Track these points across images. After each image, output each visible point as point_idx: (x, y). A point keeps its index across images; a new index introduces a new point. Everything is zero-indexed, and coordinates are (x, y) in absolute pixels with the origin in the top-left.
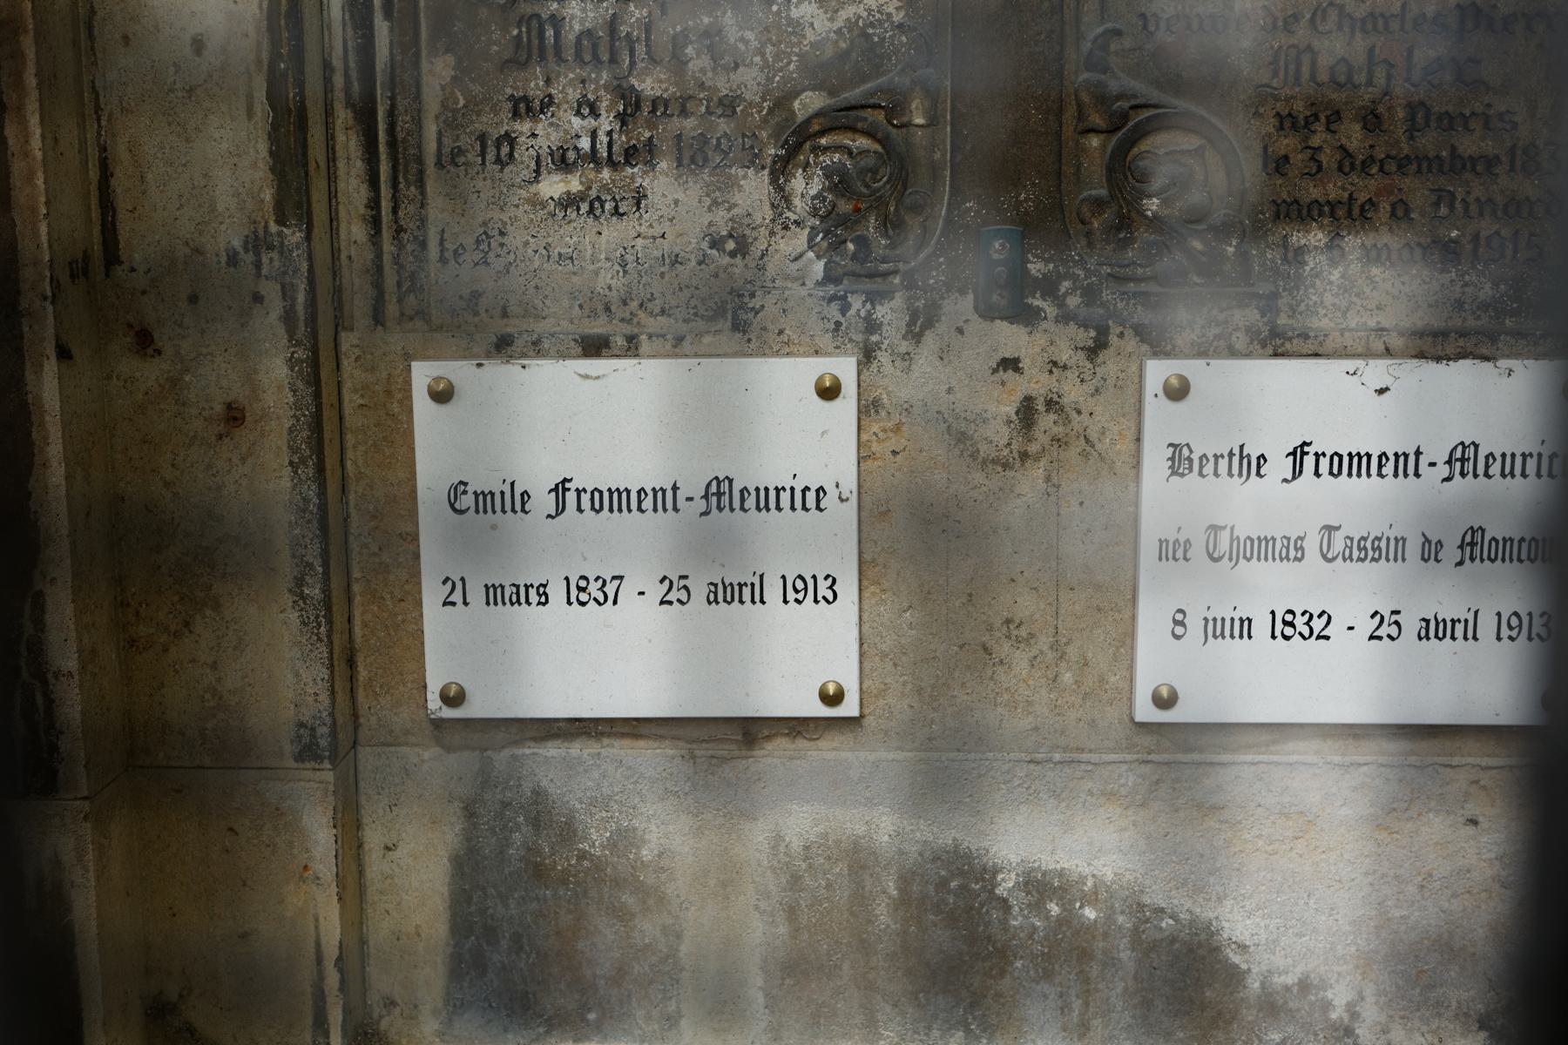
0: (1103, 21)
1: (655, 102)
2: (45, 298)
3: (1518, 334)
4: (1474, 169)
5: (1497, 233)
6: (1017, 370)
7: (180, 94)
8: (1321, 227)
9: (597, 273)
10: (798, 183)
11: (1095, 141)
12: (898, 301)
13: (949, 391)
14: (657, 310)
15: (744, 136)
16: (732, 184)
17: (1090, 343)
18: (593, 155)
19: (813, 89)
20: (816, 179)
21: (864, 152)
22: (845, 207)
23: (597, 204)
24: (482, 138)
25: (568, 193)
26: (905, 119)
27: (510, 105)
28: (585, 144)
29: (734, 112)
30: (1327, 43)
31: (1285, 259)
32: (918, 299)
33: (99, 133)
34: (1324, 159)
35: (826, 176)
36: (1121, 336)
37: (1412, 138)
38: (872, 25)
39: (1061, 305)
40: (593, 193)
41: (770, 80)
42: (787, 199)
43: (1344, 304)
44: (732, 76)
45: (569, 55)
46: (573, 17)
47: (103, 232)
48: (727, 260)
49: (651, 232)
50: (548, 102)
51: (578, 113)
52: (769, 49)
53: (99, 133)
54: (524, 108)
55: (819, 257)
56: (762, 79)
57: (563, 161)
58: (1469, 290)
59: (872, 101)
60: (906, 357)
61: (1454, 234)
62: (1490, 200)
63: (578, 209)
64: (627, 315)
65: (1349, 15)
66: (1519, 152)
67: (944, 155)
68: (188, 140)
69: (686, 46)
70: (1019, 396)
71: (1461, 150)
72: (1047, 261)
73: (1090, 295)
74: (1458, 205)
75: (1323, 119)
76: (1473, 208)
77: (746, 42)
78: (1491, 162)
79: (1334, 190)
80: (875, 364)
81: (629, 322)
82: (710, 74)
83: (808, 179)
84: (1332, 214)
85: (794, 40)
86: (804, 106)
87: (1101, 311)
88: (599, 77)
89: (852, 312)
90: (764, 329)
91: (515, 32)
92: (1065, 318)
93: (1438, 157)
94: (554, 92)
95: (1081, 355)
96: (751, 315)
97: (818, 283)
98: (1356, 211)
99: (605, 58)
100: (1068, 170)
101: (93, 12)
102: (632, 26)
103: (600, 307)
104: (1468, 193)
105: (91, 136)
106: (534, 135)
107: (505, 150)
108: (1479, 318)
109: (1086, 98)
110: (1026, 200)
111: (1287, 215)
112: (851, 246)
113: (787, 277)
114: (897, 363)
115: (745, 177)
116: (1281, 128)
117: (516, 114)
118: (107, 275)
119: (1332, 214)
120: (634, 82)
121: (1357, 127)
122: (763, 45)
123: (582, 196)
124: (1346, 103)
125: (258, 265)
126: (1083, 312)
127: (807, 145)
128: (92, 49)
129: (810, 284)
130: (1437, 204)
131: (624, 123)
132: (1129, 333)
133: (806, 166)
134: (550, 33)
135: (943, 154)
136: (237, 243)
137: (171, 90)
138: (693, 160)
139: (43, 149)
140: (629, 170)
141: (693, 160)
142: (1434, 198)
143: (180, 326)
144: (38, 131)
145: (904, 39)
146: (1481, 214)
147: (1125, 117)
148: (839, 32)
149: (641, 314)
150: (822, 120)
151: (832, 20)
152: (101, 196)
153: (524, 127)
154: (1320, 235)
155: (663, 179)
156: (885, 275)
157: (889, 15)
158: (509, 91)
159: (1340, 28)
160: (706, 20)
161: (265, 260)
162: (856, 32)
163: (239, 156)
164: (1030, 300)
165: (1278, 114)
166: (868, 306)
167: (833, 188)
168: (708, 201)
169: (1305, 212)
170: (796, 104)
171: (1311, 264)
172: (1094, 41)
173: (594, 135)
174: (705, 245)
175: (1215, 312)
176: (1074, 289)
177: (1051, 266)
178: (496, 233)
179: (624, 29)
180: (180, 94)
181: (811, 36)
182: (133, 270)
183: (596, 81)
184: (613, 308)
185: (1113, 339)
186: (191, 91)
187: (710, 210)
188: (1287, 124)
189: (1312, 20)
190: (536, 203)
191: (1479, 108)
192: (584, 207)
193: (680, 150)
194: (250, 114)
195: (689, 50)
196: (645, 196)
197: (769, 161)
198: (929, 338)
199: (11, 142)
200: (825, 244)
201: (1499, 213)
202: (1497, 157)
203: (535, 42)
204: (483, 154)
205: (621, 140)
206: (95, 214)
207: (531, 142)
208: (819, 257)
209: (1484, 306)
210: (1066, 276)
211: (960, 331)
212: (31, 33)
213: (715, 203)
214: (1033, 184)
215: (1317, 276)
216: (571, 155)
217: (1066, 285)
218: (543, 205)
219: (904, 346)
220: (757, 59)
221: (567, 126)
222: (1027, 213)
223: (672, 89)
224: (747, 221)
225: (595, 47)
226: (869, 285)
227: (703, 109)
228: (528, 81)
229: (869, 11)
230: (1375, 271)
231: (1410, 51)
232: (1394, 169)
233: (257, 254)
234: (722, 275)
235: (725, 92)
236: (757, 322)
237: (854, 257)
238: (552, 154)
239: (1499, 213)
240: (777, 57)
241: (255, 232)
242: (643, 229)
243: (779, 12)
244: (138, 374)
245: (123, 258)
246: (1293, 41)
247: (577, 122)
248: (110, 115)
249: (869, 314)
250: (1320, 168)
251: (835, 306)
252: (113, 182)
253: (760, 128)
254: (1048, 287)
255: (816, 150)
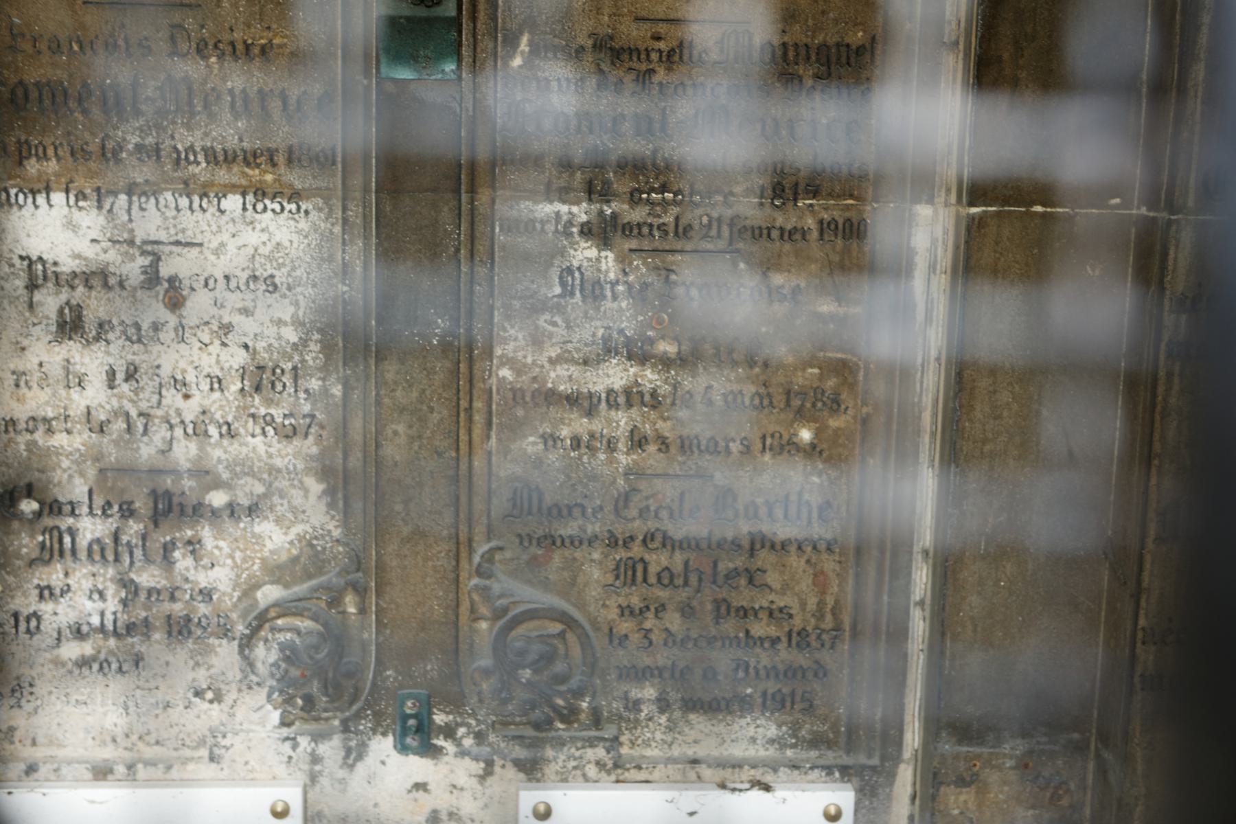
0: (489, 539)
1: (150, 592)
3: (795, 767)
4: (762, 644)
5: (780, 691)
6: (426, 790)
8: (652, 685)
9: (105, 714)
10: (260, 651)
11: (484, 625)
12: (337, 740)
13: (376, 805)
14: (153, 741)
15: (219, 616)
16: (210, 650)
17: (481, 772)
18: (102, 629)
19: (272, 583)
20: (273, 651)
21: (310, 633)
22: (295, 673)
23: (105, 665)
24: (16, 616)
25: (83, 656)
26: (341, 609)
27: (37, 592)
28: (96, 620)
29: (211, 599)
30: (654, 557)
31: (626, 708)
32: (350, 740)
34: (653, 637)
35: (282, 650)
36: (503, 766)
37: (717, 623)
38: (316, 538)
39: (459, 745)
40: (102, 656)
41: (238, 576)
42: (251, 665)
43: (669, 739)
44: (209, 572)
45: (83, 555)
46: (85, 529)
48: (206, 705)
49: (147, 685)
50: (67, 589)
51: (90, 598)
52: (238, 555)
54: (46, 593)
55: (275, 708)
56: (232, 575)
57: (78, 633)
58: (760, 730)
59: (315, 595)
60: (342, 781)
61: (749, 691)
62: (774, 667)
63: (91, 667)
64: (129, 745)
65: (671, 538)
66: (794, 635)
67: (370, 635)
69: (174, 550)
70: (427, 810)
71: (753, 632)
72: (448, 713)
73: (480, 737)
74: (751, 670)
75: (653, 609)
76: (763, 673)
77: (220, 549)
78: (775, 641)
79: (662, 658)
80: (317, 788)
81: (131, 750)
82: (192, 572)
83: (268, 649)
84: (660, 676)
85: (257, 547)
86: (265, 595)
87: (488, 749)
88: (106, 572)
89: (300, 749)
90: (234, 761)
91: (40, 538)
92: (462, 753)
93: (736, 637)
94: (70, 582)
95: (474, 781)
96: (223, 751)
97: (275, 727)
98: (677, 675)
99: (111, 558)
100: (463, 647)
102: (131, 536)
103: (108, 739)
104: (758, 662)
106: (55, 614)
107: (33, 623)
108: (767, 749)
109: (476, 597)
110: (432, 670)
111: (628, 676)
112: (300, 702)
113: (251, 722)
114: (337, 786)
115: (220, 645)
116: (622, 615)
117: (41, 596)
119: (660, 676)
120: (133, 576)
121: (677, 615)
122: (233, 551)
123: (94, 659)
124: (669, 599)
126: (475, 750)
127: (267, 626)
129: (269, 727)
130: (736, 670)
131: (125, 605)
132: (509, 765)
133: (266, 641)
134: (67, 540)
135: (370, 634)
138: (180, 633)
140: (130, 640)
141: (180, 633)
142: (734, 665)
145: (341, 549)
146: (768, 676)
147: (505, 610)
148: (291, 543)
149: (140, 745)
150: (277, 609)
151: (286, 534)
153: (47, 608)
154: (652, 691)
155: (156, 646)
156: (327, 719)
157: (329, 531)
158: (36, 581)
159: (664, 546)
160: (189, 533)
162: (304, 543)
164: (435, 741)
165: (620, 606)
166: (313, 744)
167: (287, 659)
168: (191, 663)
169: (640, 674)
170: (259, 594)
171: (646, 712)
172: (482, 557)
173: (102, 614)
174: (190, 695)
175: (573, 750)
176: (468, 734)
177: (451, 717)
178: (26, 685)
179: (124, 539)
181: (270, 545)
183: (104, 575)
184: (118, 740)
185: (497, 769)
187: (193, 669)
188: (627, 612)
189: (644, 541)
190: (58, 663)
191: (766, 604)
192: (96, 667)
193: (170, 625)
195: (177, 554)
196: (143, 659)
197: (238, 635)
198: (360, 767)
200: (280, 700)
201: (781, 677)
202: (779, 638)
203: (56, 546)
204: (16, 626)
205: (123, 618)
207: (54, 618)
208: (275, 708)
209: (772, 741)
210: (462, 725)
211: (383, 763)
213: (197, 664)
214: (437, 659)
215: (650, 719)
216: (85, 629)
217: (462, 731)
218: (63, 664)
219: (341, 773)
220: (229, 561)
221: (81, 608)
222: (432, 679)
223: (164, 582)
224: (222, 678)
225: (103, 550)
226: (313, 726)
227: (188, 597)
228: (50, 574)
229: (314, 528)
230: (692, 716)
231: (715, 564)
232: (704, 644)
234: (203, 716)
235: (203, 585)
236: (228, 756)
237: (302, 709)
238: (70, 627)
239: (781, 677)
240: (244, 560)
242: (141, 683)
243: (245, 529)
246: (630, 555)
247: (89, 605)
249: (314, 750)
250: (651, 643)
251: (288, 744)
253: (231, 611)
254: (449, 732)
255: (273, 629)
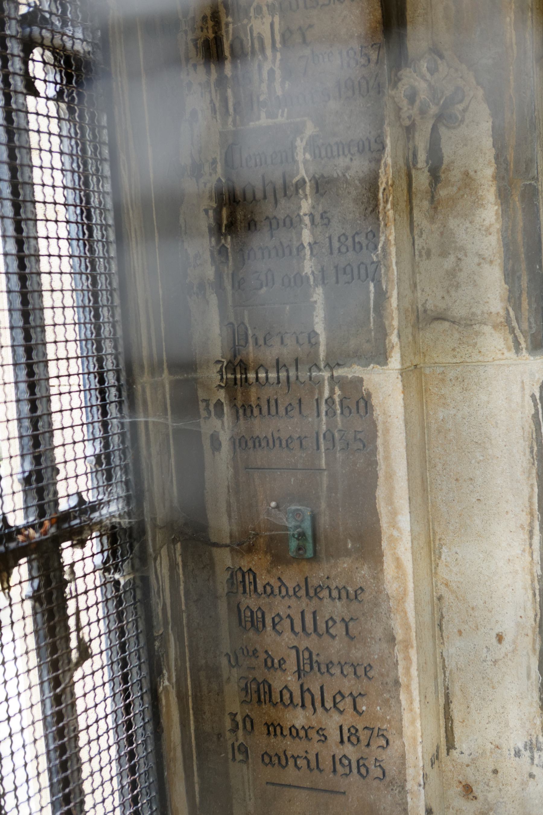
2: (420, 785)
7: (489, 663)
33: (444, 680)
47: (446, 731)
53: (444, 680)
68: (493, 688)
101: (442, 617)
105: (440, 680)
118: (448, 754)
125: (532, 759)
128: (442, 636)
136: (521, 745)
137: (485, 661)
139: (421, 708)
143: (488, 785)
144: (418, 699)
152: (445, 712)
161: (536, 755)
163: (522, 698)
180: (489, 663)
182: (462, 753)
186: (495, 662)
194: (529, 677)
199: (403, 702)
206: (442, 722)
212: (415, 648)
233: (532, 751)
241: (531, 741)
244: (464, 808)
245: (457, 746)
248: (451, 671)
252: (452, 706)
